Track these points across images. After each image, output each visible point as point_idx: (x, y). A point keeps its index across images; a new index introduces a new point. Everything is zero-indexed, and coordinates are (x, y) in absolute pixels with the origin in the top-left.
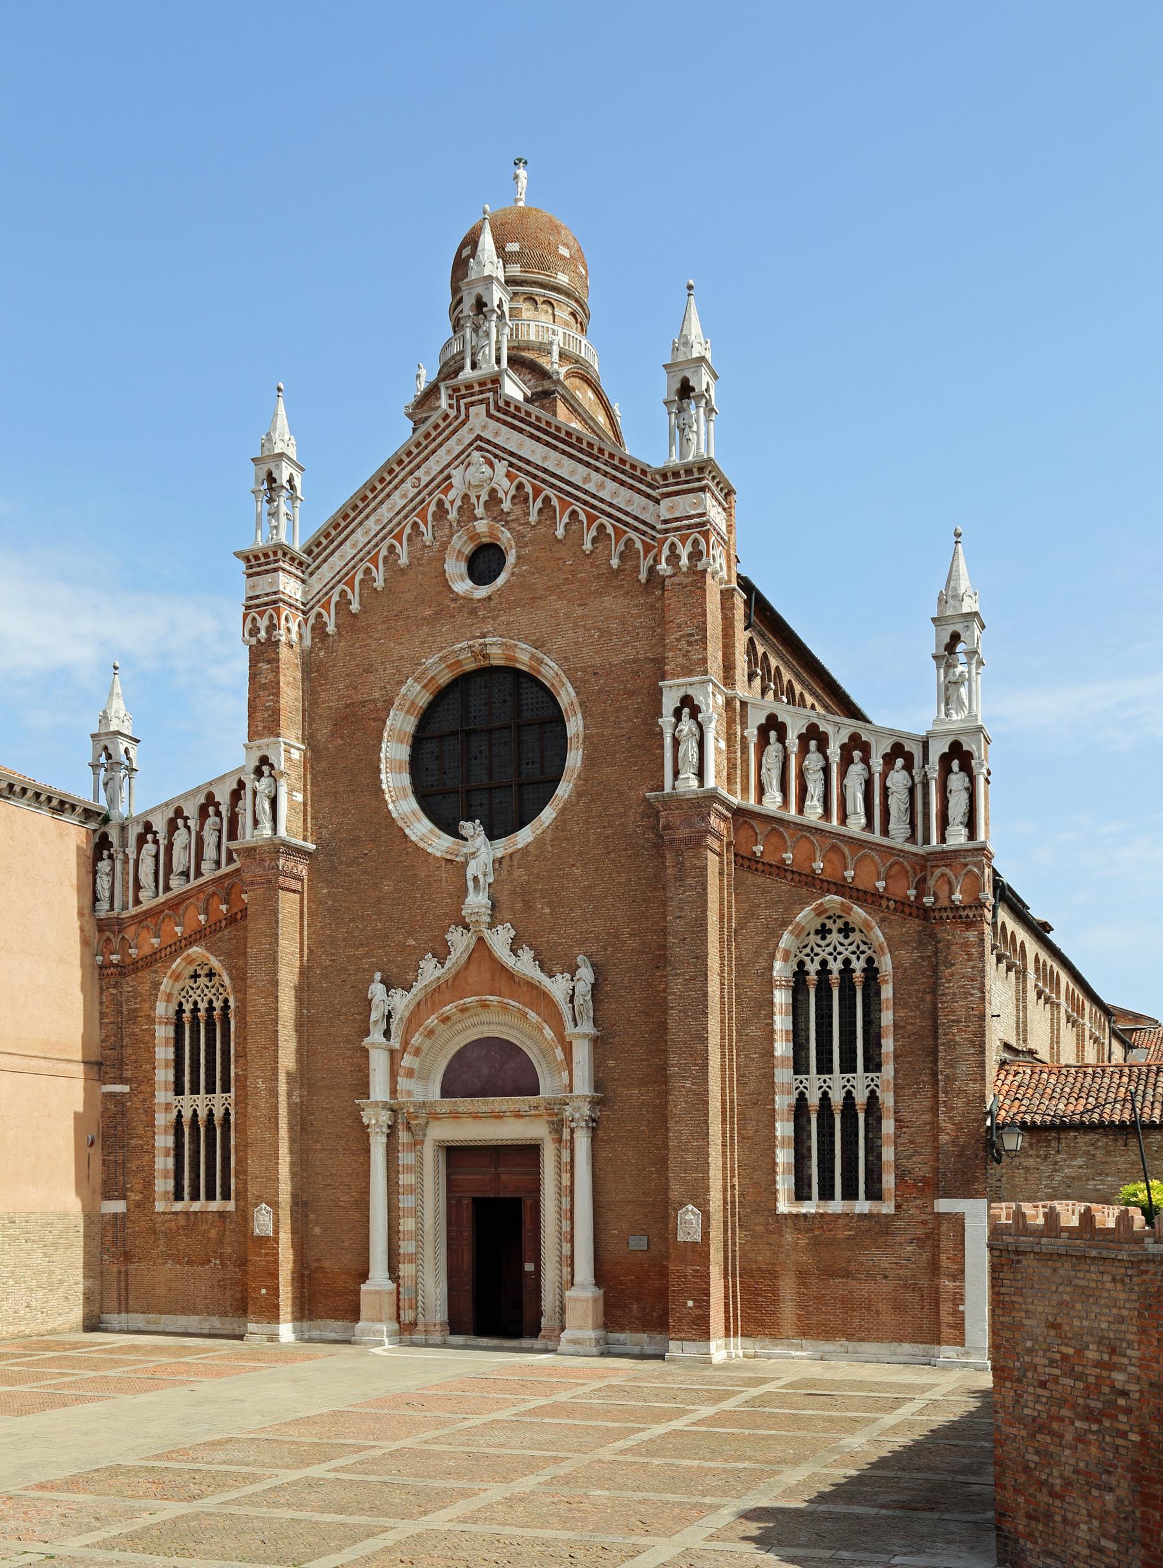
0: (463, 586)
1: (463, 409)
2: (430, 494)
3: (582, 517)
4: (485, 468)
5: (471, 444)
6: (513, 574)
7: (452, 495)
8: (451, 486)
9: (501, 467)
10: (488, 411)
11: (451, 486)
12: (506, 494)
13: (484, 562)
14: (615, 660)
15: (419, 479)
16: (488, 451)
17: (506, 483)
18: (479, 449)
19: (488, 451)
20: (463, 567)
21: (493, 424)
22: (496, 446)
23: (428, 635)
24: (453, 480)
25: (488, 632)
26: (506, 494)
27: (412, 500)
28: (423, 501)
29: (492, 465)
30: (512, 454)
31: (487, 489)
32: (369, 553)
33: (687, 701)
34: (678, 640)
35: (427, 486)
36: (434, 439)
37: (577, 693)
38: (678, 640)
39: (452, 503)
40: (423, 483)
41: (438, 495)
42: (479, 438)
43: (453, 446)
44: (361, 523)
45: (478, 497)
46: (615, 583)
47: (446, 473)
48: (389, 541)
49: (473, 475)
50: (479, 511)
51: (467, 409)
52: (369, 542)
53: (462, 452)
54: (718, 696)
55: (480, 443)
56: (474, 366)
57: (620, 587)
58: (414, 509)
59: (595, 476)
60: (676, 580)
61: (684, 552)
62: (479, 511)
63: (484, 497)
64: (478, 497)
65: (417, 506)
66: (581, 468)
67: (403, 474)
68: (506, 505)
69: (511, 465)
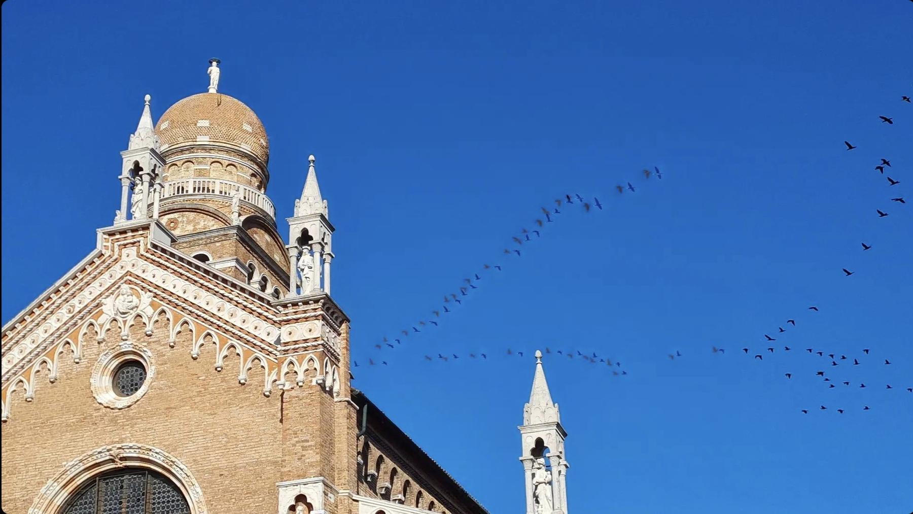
0: (108, 396)
1: (116, 249)
2: (82, 318)
3: (216, 339)
4: (134, 298)
5: (121, 278)
6: (151, 387)
7: (101, 320)
8: (101, 312)
9: (146, 298)
10: (138, 252)
11: (101, 312)
12: (150, 319)
13: (128, 374)
14: (240, 462)
15: (73, 307)
16: (136, 284)
17: (150, 311)
18: (130, 282)
19: (136, 284)
20: (107, 381)
21: (141, 262)
22: (144, 280)
23: (71, 440)
24: (103, 307)
25: (125, 438)
26: (150, 319)
27: (65, 324)
28: (75, 324)
29: (139, 297)
30: (157, 287)
31: (133, 313)
32: (22, 367)
33: (301, 498)
34: (294, 445)
35: (80, 312)
36: (89, 274)
37: (204, 493)
38: (294, 445)
39: (101, 326)
40: (77, 310)
41: (89, 319)
42: (129, 273)
43: (106, 280)
44: (17, 342)
45: (125, 322)
46: (242, 396)
47: (97, 301)
48: (42, 357)
49: (122, 303)
50: (125, 331)
51: (120, 250)
52: (23, 359)
53: (113, 285)
54: (330, 495)
55: (131, 279)
56: (129, 216)
57: (246, 399)
58: (67, 331)
59: (229, 306)
60: (293, 393)
61: (300, 369)
62: (125, 331)
63: (130, 320)
64: (125, 322)
65: (71, 326)
66: (216, 300)
67: (59, 301)
68: (149, 328)
69: (156, 296)
